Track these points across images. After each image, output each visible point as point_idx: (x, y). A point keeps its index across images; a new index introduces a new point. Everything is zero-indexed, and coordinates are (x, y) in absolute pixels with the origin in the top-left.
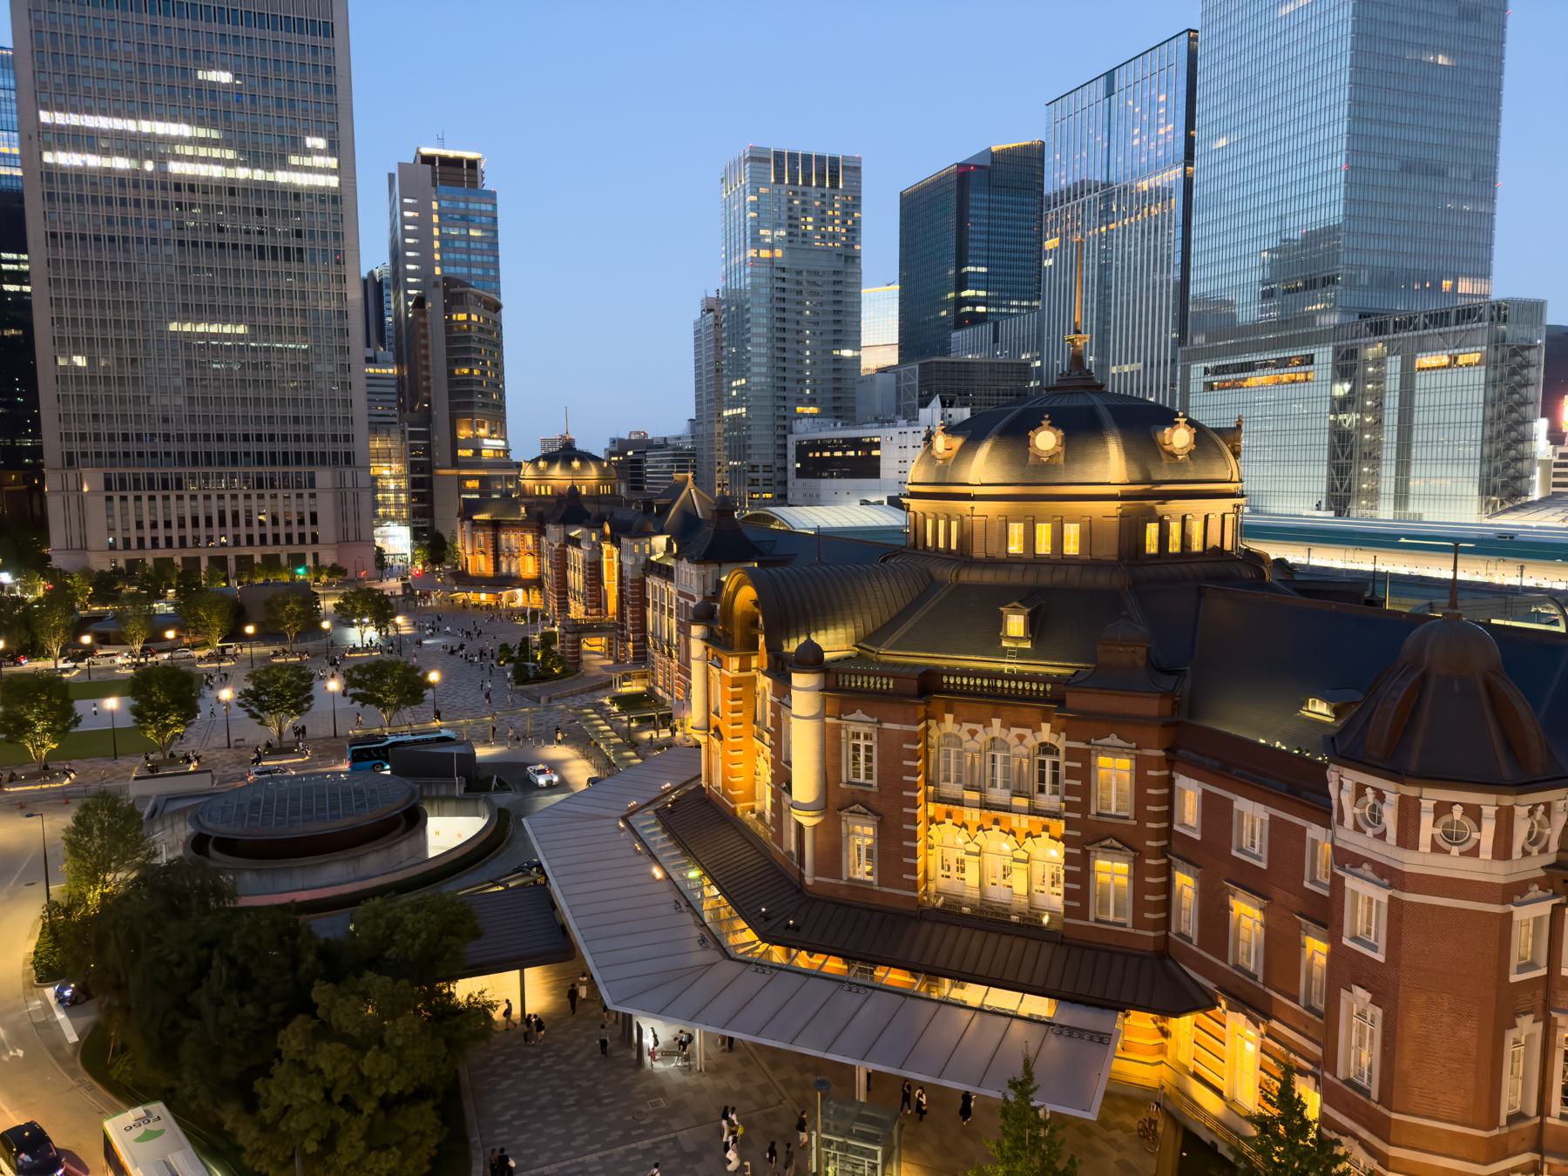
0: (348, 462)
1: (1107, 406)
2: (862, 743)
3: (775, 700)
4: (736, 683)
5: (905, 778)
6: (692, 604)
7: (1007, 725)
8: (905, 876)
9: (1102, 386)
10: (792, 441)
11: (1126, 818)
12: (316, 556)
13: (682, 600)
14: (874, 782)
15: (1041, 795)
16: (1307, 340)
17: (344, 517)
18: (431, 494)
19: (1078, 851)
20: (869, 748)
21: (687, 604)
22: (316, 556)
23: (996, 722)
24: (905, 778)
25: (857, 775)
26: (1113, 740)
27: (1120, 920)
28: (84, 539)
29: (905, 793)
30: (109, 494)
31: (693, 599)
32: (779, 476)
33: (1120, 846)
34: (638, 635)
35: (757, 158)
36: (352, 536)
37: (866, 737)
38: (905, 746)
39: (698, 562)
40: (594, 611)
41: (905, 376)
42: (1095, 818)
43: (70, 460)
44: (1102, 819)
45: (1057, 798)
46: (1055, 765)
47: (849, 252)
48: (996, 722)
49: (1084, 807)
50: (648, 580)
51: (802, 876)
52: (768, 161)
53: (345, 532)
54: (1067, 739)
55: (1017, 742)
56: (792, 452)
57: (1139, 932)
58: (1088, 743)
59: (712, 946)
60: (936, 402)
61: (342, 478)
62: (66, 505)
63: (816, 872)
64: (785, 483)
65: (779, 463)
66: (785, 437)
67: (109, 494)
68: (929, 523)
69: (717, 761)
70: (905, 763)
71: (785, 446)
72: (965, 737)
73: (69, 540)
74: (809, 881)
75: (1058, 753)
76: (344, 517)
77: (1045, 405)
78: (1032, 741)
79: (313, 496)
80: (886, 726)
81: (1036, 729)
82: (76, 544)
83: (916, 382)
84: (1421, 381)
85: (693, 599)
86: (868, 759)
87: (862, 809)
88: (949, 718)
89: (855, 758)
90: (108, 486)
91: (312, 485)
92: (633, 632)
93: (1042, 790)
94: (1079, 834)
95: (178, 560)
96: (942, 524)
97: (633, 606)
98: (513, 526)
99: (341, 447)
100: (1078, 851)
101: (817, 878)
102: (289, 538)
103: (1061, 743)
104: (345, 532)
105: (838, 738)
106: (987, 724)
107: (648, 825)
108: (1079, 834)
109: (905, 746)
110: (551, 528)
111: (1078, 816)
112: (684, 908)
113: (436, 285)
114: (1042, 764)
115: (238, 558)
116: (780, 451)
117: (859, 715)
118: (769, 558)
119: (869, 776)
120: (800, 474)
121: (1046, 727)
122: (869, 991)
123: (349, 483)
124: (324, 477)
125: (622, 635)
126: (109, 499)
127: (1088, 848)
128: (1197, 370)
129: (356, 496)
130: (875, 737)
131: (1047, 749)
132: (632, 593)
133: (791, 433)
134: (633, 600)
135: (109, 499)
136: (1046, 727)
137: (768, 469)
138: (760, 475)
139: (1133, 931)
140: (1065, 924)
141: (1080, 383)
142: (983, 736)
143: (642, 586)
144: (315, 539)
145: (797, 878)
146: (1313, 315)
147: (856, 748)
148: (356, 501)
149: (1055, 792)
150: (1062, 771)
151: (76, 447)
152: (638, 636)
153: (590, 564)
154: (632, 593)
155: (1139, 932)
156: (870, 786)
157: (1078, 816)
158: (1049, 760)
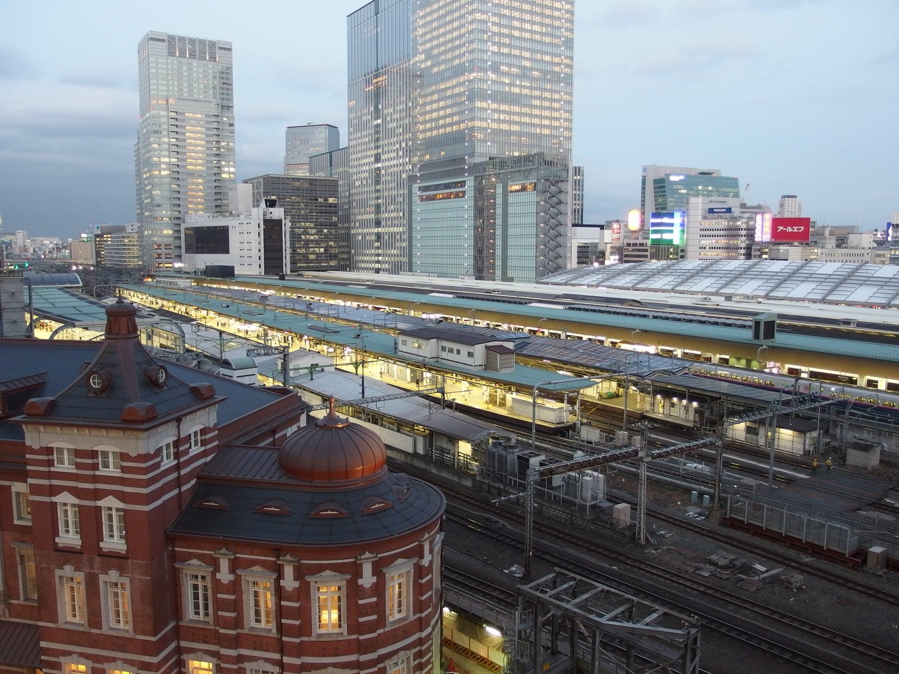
10: (183, 227)
16: (461, 172)
32: (177, 252)
35: (153, 39)
47: (226, 103)
52: (163, 40)
56: (183, 236)
65: (177, 243)
83: (262, 190)
84: (511, 199)
120: (187, 252)
128: (415, 187)
133: (184, 222)
137: (167, 246)
138: (163, 251)
146: (177, 173)
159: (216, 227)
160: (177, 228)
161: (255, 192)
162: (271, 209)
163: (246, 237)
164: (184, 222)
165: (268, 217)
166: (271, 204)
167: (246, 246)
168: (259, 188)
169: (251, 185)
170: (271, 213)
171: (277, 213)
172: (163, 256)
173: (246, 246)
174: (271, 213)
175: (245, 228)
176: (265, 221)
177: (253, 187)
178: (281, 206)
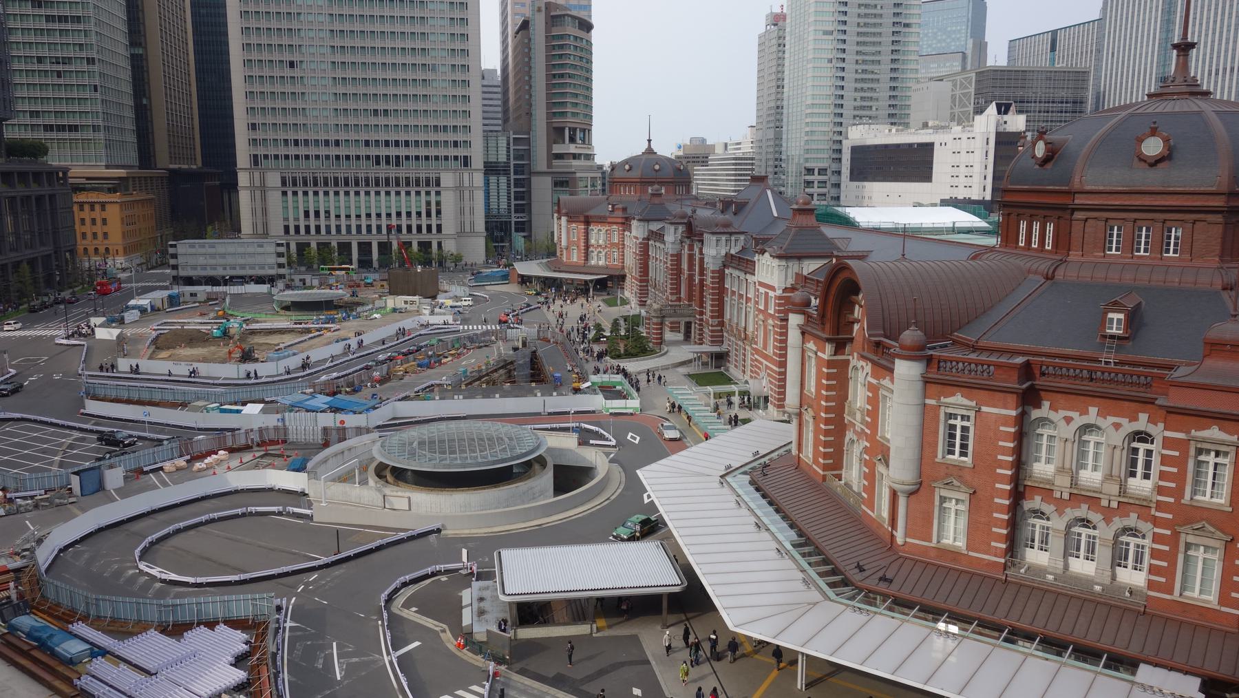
0: (466, 165)
1: (1217, 112)
2: (959, 423)
3: (874, 381)
4: (830, 364)
5: (1000, 457)
6: (771, 294)
7: (1102, 414)
8: (993, 544)
9: (1207, 93)
11: (1222, 505)
12: (440, 244)
13: (762, 290)
14: (968, 460)
15: (1131, 481)
17: (462, 212)
18: (529, 192)
19: (1168, 532)
20: (965, 429)
21: (767, 294)
22: (440, 244)
23: (1093, 411)
24: (1000, 457)
25: (952, 453)
26: (1214, 433)
27: (1204, 597)
28: (265, 225)
29: (999, 471)
30: (285, 189)
31: (773, 289)
32: (834, 179)
33: (1212, 530)
34: (716, 321)
36: (467, 229)
37: (963, 417)
38: (1002, 428)
39: (780, 257)
40: (674, 298)
41: (962, 84)
42: (1187, 503)
43: (255, 159)
44: (1195, 504)
45: (1148, 485)
46: (1149, 453)
48: (1093, 411)
49: (1178, 493)
50: (727, 271)
51: (892, 536)
53: (462, 224)
54: (1166, 429)
55: (1112, 429)
57: (1223, 609)
58: (1188, 432)
59: (813, 588)
60: (992, 109)
61: (461, 180)
62: (253, 199)
63: (906, 535)
64: (838, 186)
65: (834, 167)
66: (841, 141)
67: (285, 189)
68: (1023, 226)
69: (807, 434)
70: (1001, 443)
71: (840, 151)
72: (1063, 423)
73: (255, 225)
74: (900, 540)
75: (1152, 443)
76: (462, 212)
77: (1148, 111)
78: (1129, 427)
79: (438, 193)
80: (984, 409)
81: (1134, 418)
82: (260, 231)
83: (972, 90)
85: (773, 288)
86: (964, 438)
87: (955, 482)
88: (1046, 404)
89: (952, 436)
90: (284, 183)
91: (438, 184)
92: (712, 317)
93: (1133, 474)
94: (1170, 516)
95: (334, 244)
96: (1036, 227)
97: (713, 294)
98: (602, 220)
99: (461, 152)
100: (1168, 532)
101: (908, 540)
102: (419, 228)
103: (1157, 430)
104: (462, 224)
105: (938, 416)
106: (1084, 412)
107: (741, 482)
108: (1170, 516)
109: (1002, 428)
110: (634, 223)
111: (1172, 500)
112: (784, 554)
113: (539, 10)
114: (1136, 451)
115: (380, 244)
116: (835, 156)
117: (958, 399)
118: (845, 255)
119: (963, 454)
121: (1143, 417)
122: (961, 638)
123: (466, 184)
124: (447, 179)
125: (701, 320)
126: (284, 193)
127: (1178, 529)
129: (471, 193)
130: (972, 418)
131: (1142, 437)
132: (713, 283)
134: (713, 288)
135: (284, 193)
136: (1143, 417)
137: (822, 171)
139: (1218, 608)
140: (1148, 598)
141: (1184, 89)
142: (1079, 420)
143: (720, 276)
144: (439, 228)
145: (888, 538)
147: (953, 427)
148: (472, 198)
149: (1147, 476)
150: (1156, 459)
151: (261, 151)
152: (716, 321)
153: (672, 255)
154: (713, 283)
155: (1223, 609)
156: (964, 462)
157: (1172, 500)
158: (1142, 447)
159: (898, 146)
160: (836, 147)
161: (958, 92)
162: (1006, 118)
163: (964, 159)
164: (847, 138)
165: (1001, 129)
166: (1003, 109)
167: (963, 171)
168: (966, 88)
169: (950, 83)
170: (1005, 122)
171: (1017, 122)
172: (816, 184)
173: (963, 171)
174: (1005, 122)
175: (964, 145)
176: (998, 134)
177: (955, 85)
178: (1020, 112)
